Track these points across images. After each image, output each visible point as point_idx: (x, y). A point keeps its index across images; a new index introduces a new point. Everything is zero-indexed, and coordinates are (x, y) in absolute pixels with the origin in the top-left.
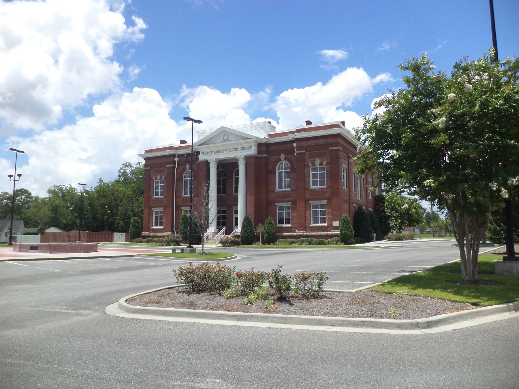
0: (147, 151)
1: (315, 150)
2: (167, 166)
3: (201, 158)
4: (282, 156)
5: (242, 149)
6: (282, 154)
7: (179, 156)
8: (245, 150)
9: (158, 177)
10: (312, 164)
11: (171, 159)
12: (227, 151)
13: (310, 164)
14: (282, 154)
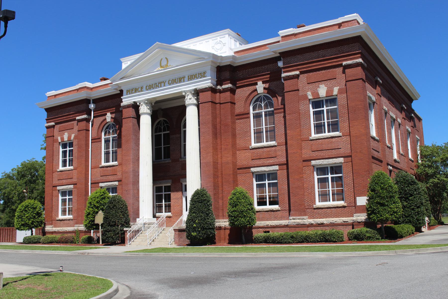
6: (260, 83)
14: (260, 83)
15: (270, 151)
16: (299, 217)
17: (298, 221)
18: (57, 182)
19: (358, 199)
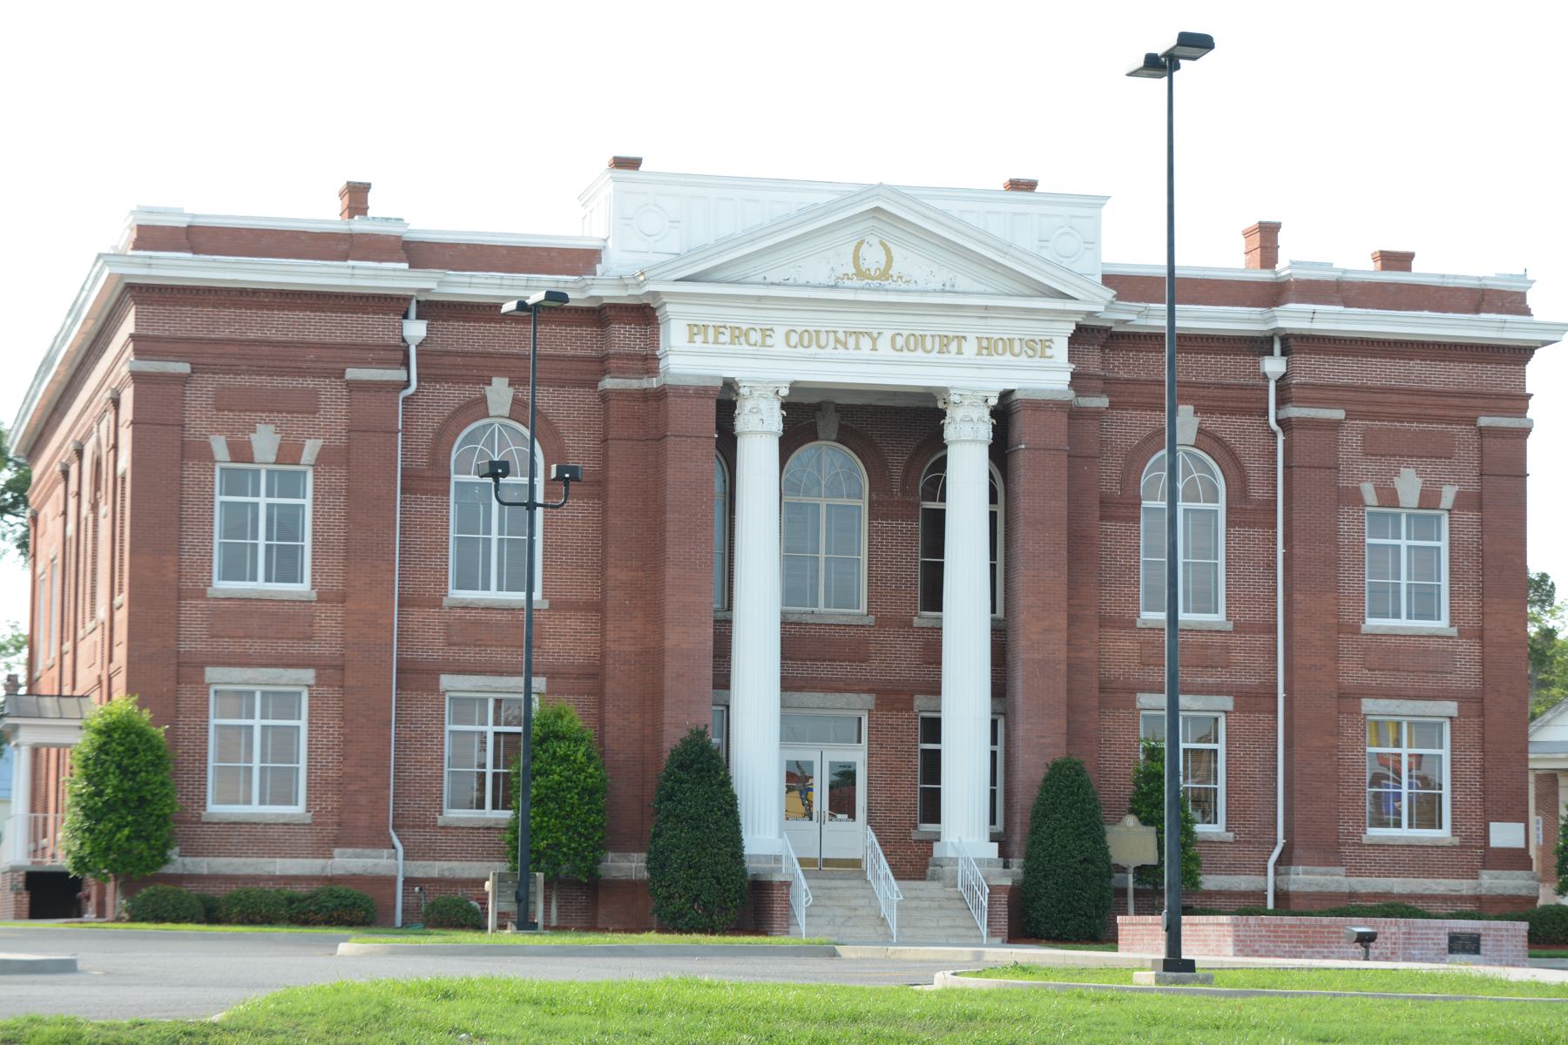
0: (150, 237)
1: (1400, 418)
2: (352, 373)
3: (686, 356)
4: (1187, 422)
5: (988, 347)
7: (432, 310)
9: (265, 441)
10: (1379, 490)
11: (373, 328)
12: (884, 344)
13: (1368, 491)
14: (1186, 412)
15: (1205, 647)
17: (1323, 878)
18: (201, 647)
19: (1494, 826)
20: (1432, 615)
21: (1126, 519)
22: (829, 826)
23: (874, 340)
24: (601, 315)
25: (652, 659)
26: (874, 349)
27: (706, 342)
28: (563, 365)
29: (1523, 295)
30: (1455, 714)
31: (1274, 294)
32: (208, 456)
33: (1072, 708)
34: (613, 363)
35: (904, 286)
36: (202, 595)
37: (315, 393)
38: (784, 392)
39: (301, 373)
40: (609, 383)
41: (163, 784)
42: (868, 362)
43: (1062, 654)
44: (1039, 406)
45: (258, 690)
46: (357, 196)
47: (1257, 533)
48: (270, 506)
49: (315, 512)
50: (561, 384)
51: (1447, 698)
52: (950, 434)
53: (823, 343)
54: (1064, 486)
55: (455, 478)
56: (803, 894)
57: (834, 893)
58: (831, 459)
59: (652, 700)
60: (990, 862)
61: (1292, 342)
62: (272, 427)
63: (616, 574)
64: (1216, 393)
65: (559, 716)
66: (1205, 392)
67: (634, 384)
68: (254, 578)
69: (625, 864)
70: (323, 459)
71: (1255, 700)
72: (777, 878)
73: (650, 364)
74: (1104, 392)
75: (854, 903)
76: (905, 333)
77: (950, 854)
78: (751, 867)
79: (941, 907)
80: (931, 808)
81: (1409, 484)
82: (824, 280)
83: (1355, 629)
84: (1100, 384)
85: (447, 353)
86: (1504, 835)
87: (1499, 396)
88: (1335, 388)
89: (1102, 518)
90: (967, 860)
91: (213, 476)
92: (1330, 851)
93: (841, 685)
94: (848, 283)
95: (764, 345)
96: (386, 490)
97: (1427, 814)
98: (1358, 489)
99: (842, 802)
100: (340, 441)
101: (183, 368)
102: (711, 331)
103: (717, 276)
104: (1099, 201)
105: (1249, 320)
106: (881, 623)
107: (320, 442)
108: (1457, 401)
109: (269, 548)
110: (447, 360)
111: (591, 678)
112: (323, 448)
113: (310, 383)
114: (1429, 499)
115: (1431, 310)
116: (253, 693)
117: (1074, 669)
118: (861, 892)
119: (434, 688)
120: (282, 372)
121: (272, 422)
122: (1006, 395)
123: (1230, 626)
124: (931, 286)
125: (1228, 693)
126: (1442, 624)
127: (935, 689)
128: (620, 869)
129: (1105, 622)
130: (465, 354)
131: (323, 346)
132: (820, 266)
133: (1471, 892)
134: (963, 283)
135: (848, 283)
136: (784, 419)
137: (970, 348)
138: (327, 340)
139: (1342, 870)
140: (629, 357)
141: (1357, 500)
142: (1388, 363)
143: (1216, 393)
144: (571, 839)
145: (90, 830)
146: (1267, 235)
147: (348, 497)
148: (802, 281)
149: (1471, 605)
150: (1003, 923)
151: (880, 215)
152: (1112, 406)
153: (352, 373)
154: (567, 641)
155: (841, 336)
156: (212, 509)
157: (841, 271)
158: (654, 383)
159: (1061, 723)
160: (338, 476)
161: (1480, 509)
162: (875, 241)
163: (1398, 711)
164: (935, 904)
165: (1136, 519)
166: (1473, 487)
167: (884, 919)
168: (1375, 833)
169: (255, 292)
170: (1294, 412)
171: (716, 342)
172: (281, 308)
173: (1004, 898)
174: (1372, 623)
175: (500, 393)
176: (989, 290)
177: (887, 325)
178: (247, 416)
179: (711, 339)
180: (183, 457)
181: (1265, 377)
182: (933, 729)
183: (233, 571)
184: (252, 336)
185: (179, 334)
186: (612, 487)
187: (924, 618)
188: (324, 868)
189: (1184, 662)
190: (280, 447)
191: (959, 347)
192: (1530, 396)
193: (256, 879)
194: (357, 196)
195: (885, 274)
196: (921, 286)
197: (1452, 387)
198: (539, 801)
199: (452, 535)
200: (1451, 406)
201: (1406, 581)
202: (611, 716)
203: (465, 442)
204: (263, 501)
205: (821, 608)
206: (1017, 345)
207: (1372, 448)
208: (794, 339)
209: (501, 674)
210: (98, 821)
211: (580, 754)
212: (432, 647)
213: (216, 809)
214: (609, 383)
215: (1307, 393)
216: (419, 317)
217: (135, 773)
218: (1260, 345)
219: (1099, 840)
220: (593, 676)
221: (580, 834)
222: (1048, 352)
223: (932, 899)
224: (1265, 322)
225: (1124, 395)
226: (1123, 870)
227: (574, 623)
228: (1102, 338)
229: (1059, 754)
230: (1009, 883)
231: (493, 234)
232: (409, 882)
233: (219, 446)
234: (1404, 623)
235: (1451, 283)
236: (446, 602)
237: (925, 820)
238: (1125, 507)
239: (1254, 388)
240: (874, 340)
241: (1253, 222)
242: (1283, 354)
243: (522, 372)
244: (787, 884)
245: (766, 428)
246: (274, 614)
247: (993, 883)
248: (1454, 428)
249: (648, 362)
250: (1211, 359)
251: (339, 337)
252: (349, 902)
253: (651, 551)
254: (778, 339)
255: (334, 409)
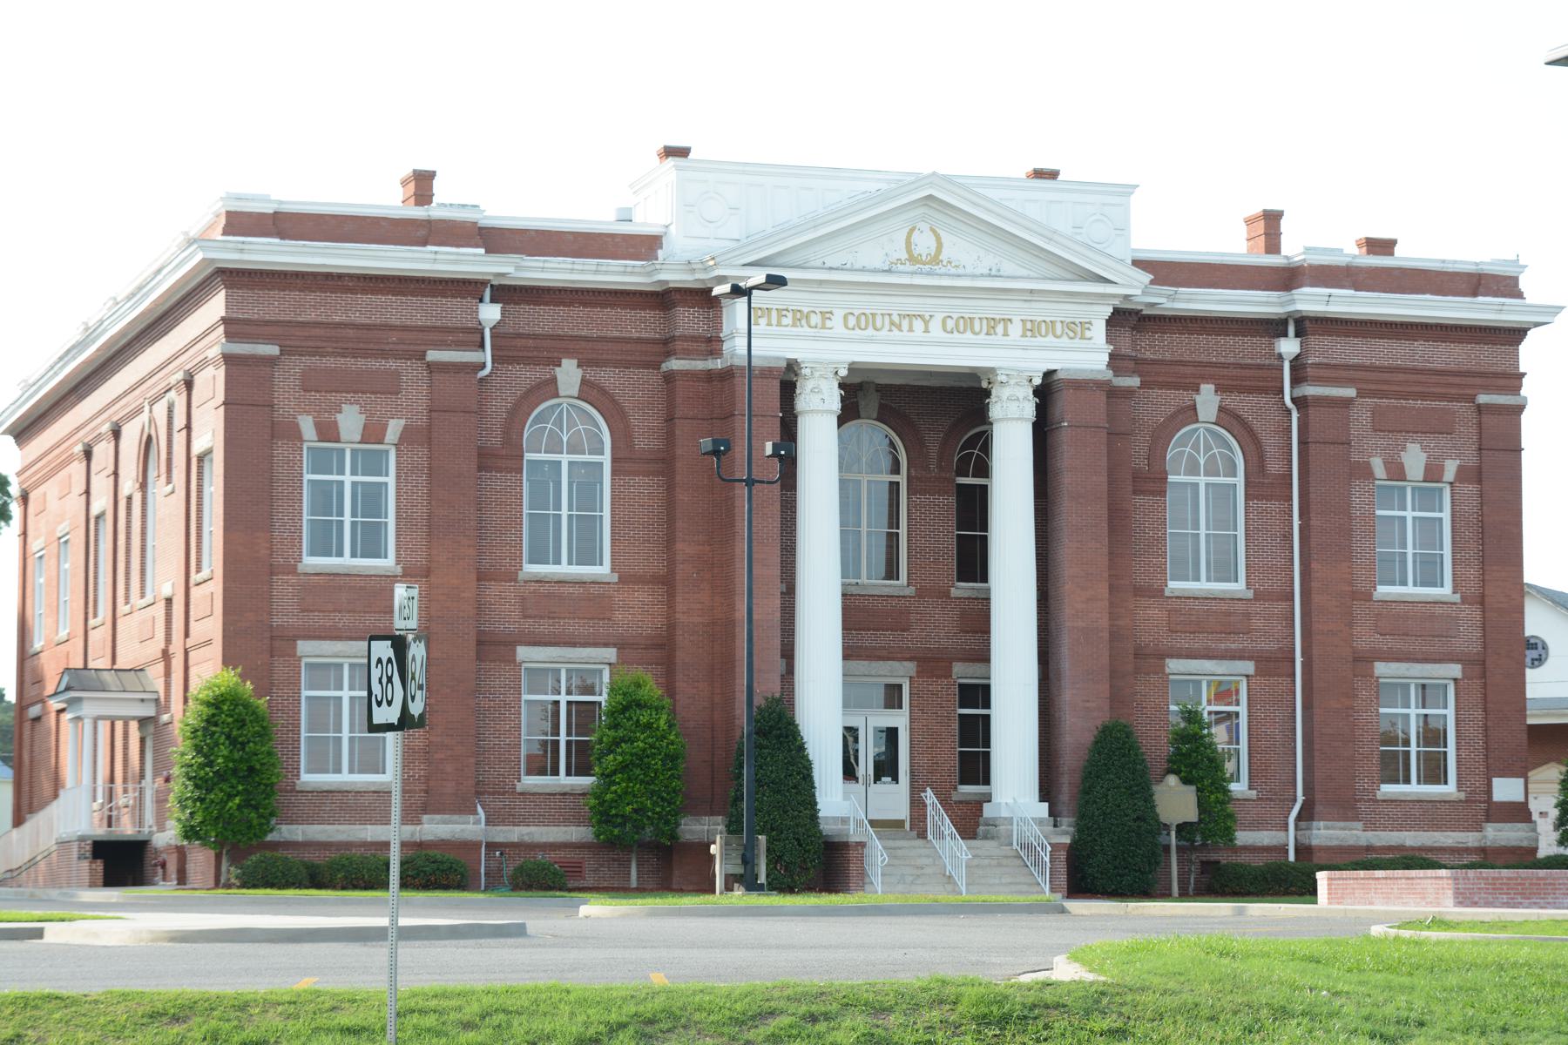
0: (239, 223)
2: (433, 355)
3: (755, 337)
4: (1208, 400)
5: (1032, 329)
6: (1207, 389)
7: (506, 293)
8: (1050, 340)
9: (350, 421)
11: (450, 311)
13: (1378, 465)
14: (1207, 389)
16: (1342, 824)
19: (1496, 781)
20: (1436, 582)
21: (1153, 493)
22: (874, 788)
23: (926, 323)
24: (664, 299)
25: (721, 631)
26: (927, 331)
27: (769, 324)
28: (629, 347)
29: (1516, 279)
30: (1459, 675)
31: (1289, 278)
32: (295, 435)
33: (1114, 674)
34: (679, 345)
35: (953, 271)
36: (293, 570)
37: (397, 374)
38: (843, 372)
39: (384, 354)
40: (675, 364)
41: (269, 754)
42: (921, 343)
43: (1104, 622)
44: (1080, 385)
45: (346, 663)
46: (422, 184)
47: (1274, 506)
48: (354, 484)
49: (398, 489)
50: (627, 365)
51: (1452, 661)
52: (995, 412)
53: (879, 325)
54: (1104, 462)
55: (528, 456)
56: (877, 854)
57: (899, 853)
58: (874, 435)
59: (722, 668)
60: (1040, 822)
61: (1307, 324)
62: (357, 407)
63: (684, 548)
64: (1235, 372)
65: (639, 686)
66: (1225, 372)
67: (700, 365)
68: (340, 554)
69: (698, 827)
70: (406, 437)
71: (1273, 664)
72: (854, 839)
73: (715, 345)
74: (1134, 372)
75: (920, 862)
76: (955, 316)
77: (1004, 814)
78: (826, 828)
79: (999, 865)
80: (976, 767)
81: (1414, 459)
82: (878, 264)
83: (1368, 597)
84: (1131, 365)
85: (519, 336)
86: (1506, 789)
87: (1496, 375)
88: (1347, 367)
89: (1135, 492)
90: (1024, 820)
91: (301, 455)
92: (1347, 807)
93: (884, 653)
94: (901, 268)
95: (823, 327)
96: (467, 466)
97: (1434, 772)
98: (1368, 463)
99: (886, 768)
100: (422, 421)
101: (273, 350)
102: (774, 313)
103: (780, 261)
104: (1128, 190)
105: (1267, 304)
106: (921, 593)
107: (403, 422)
108: (1457, 380)
109: (354, 524)
110: (520, 342)
111: (661, 650)
112: (406, 428)
113: (392, 364)
114: (1433, 473)
115: (1433, 293)
116: (341, 666)
117: (1115, 636)
118: (923, 851)
119: (511, 659)
120: (366, 354)
121: (357, 402)
122: (1048, 375)
123: (1250, 594)
124: (978, 271)
125: (1250, 658)
126: (1445, 591)
127: (984, 657)
128: (692, 832)
129: (1139, 591)
130: (535, 337)
131: (405, 328)
132: (875, 252)
133: (1476, 844)
134: (1008, 268)
135: (901, 268)
136: (843, 399)
137: (1015, 330)
138: (409, 323)
139: (1360, 825)
140: (694, 339)
141: (1367, 473)
142: (1394, 344)
143: (1235, 372)
144: (655, 804)
145: (202, 800)
146: (1272, 220)
147: (430, 475)
148: (857, 266)
149: (1473, 572)
150: (1063, 879)
151: (934, 203)
152: (1144, 385)
153: (433, 355)
154: (638, 612)
155: (896, 319)
156: (301, 487)
157: (896, 256)
158: (718, 364)
159: (1104, 688)
160: (420, 455)
161: (1480, 481)
162: (924, 226)
163: (1408, 674)
164: (994, 862)
165: (1163, 493)
166: (1472, 461)
167: (950, 877)
168: (1388, 789)
169: (340, 276)
170: (1310, 390)
171: (779, 324)
172: (364, 291)
173: (1063, 855)
174: (1383, 591)
175: (569, 374)
176: (1032, 274)
177: (938, 308)
178: (333, 397)
179: (774, 321)
180: (273, 437)
181: (1280, 357)
182: (979, 694)
183: (325, 546)
184: (337, 319)
185: (267, 317)
186: (679, 465)
187: (963, 589)
188: (413, 834)
189: (1211, 626)
190: (365, 427)
191: (1006, 329)
192: (1523, 375)
193: (348, 845)
194: (422, 184)
195: (935, 260)
196: (969, 270)
197: (1453, 367)
198: (624, 768)
199: (525, 511)
200: (1451, 385)
201: (1412, 549)
202: (681, 685)
203: (535, 422)
204: (348, 479)
205: (864, 580)
206: (1059, 326)
207: (1381, 424)
208: (852, 321)
209: (574, 645)
210: (209, 791)
211: (662, 722)
212: (507, 618)
213: (308, 779)
214: (675, 364)
215: (1322, 373)
216: (493, 301)
217: (243, 744)
218: (1275, 327)
219: (1148, 799)
220: (661, 646)
221: (663, 799)
222: (1088, 334)
223: (987, 857)
224: (1282, 304)
225: (1156, 375)
226: (1167, 827)
227: (642, 596)
228: (1133, 320)
229: (1102, 717)
230: (1067, 840)
231: (561, 221)
232: (491, 846)
233: (307, 426)
234: (1411, 590)
235: (1450, 268)
236: (521, 576)
237: (964, 781)
238: (1153, 482)
239: (1269, 367)
240: (926, 323)
241: (1257, 209)
242: (1297, 335)
243: (591, 354)
244: (862, 845)
245: (826, 407)
246: (361, 588)
247: (1054, 841)
248: (1455, 406)
249: (712, 344)
250: (1230, 340)
251: (419, 319)
252: (445, 866)
253: (720, 526)
254: (837, 321)
255: (415, 390)
